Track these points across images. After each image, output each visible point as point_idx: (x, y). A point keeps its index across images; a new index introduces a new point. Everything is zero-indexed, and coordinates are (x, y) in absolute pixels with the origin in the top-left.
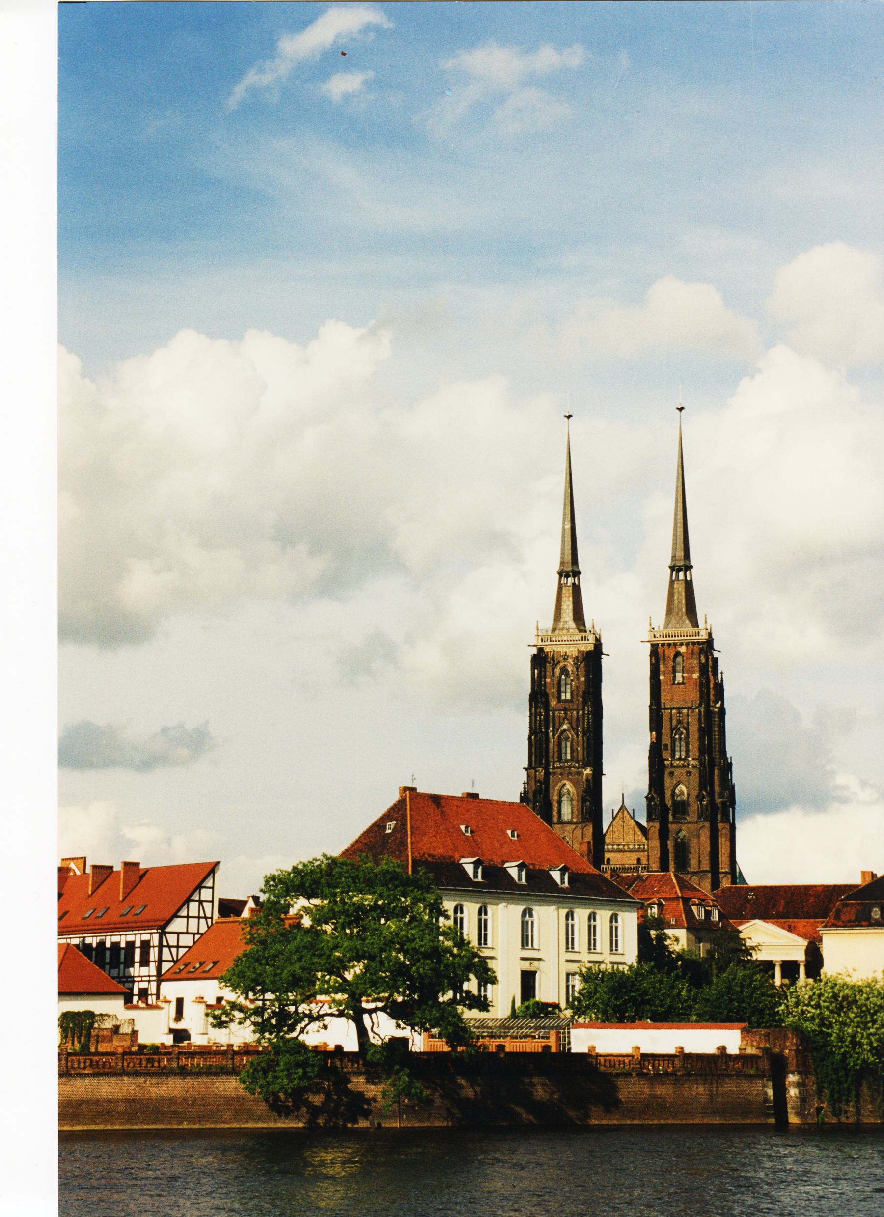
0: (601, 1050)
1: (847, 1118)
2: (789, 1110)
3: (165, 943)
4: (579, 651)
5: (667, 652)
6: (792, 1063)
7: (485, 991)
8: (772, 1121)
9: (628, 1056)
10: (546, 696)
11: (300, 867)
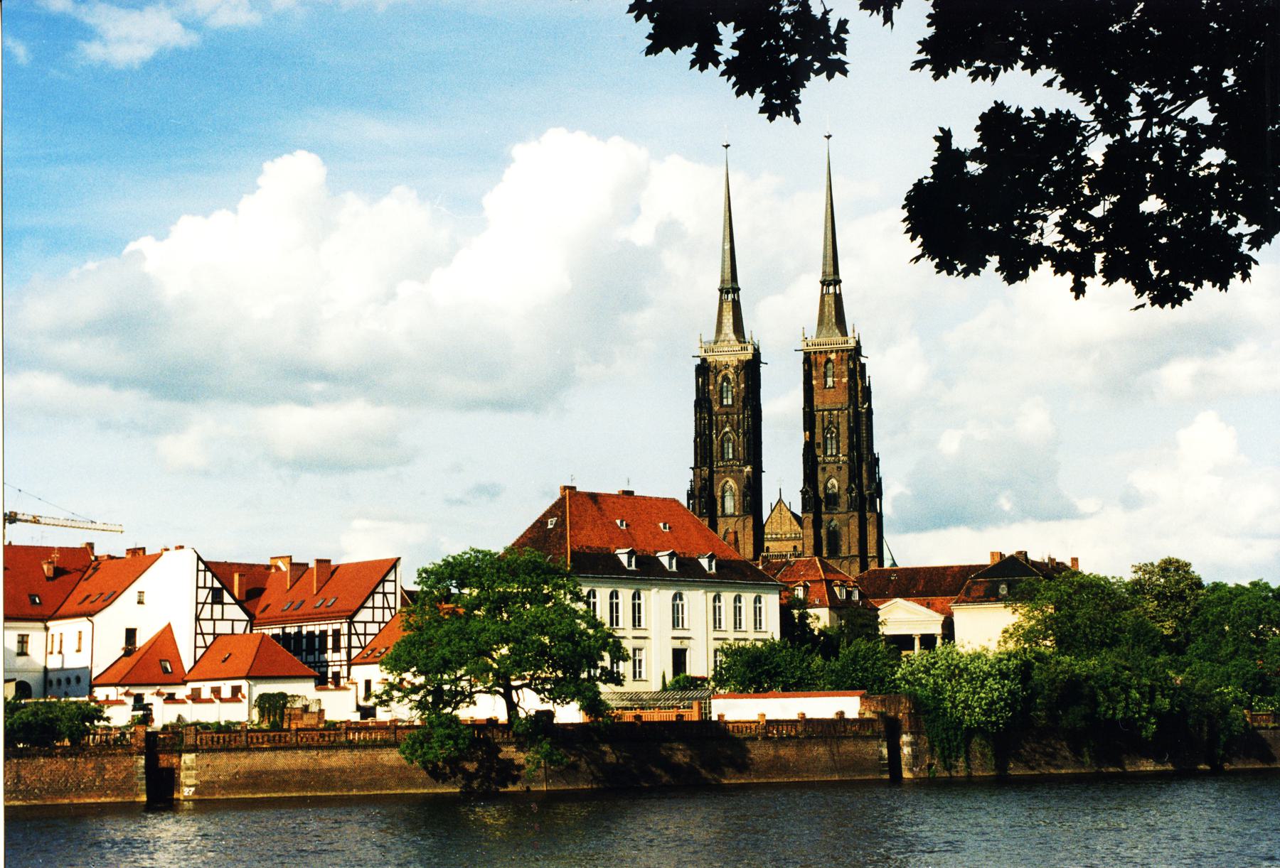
0: (728, 718)
1: (957, 772)
2: (903, 767)
3: (353, 631)
4: (739, 361)
5: (819, 359)
6: (906, 727)
7: (618, 667)
8: (887, 776)
9: (754, 722)
10: (710, 402)
11: (451, 560)
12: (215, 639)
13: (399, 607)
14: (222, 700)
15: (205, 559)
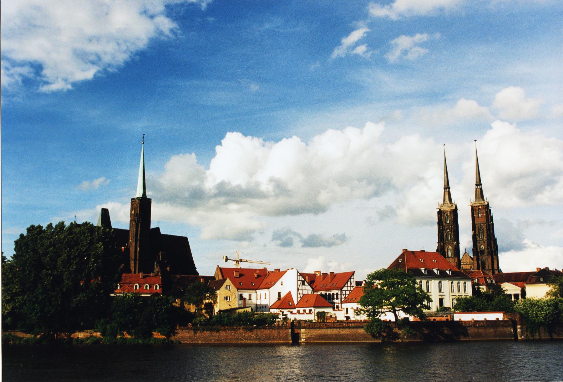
0: (463, 320)
1: (536, 337)
2: (518, 335)
3: (342, 293)
4: (451, 210)
6: (519, 323)
7: (429, 304)
8: (513, 338)
9: (470, 321)
11: (377, 272)
12: (303, 295)
13: (355, 286)
14: (307, 314)
15: (300, 272)
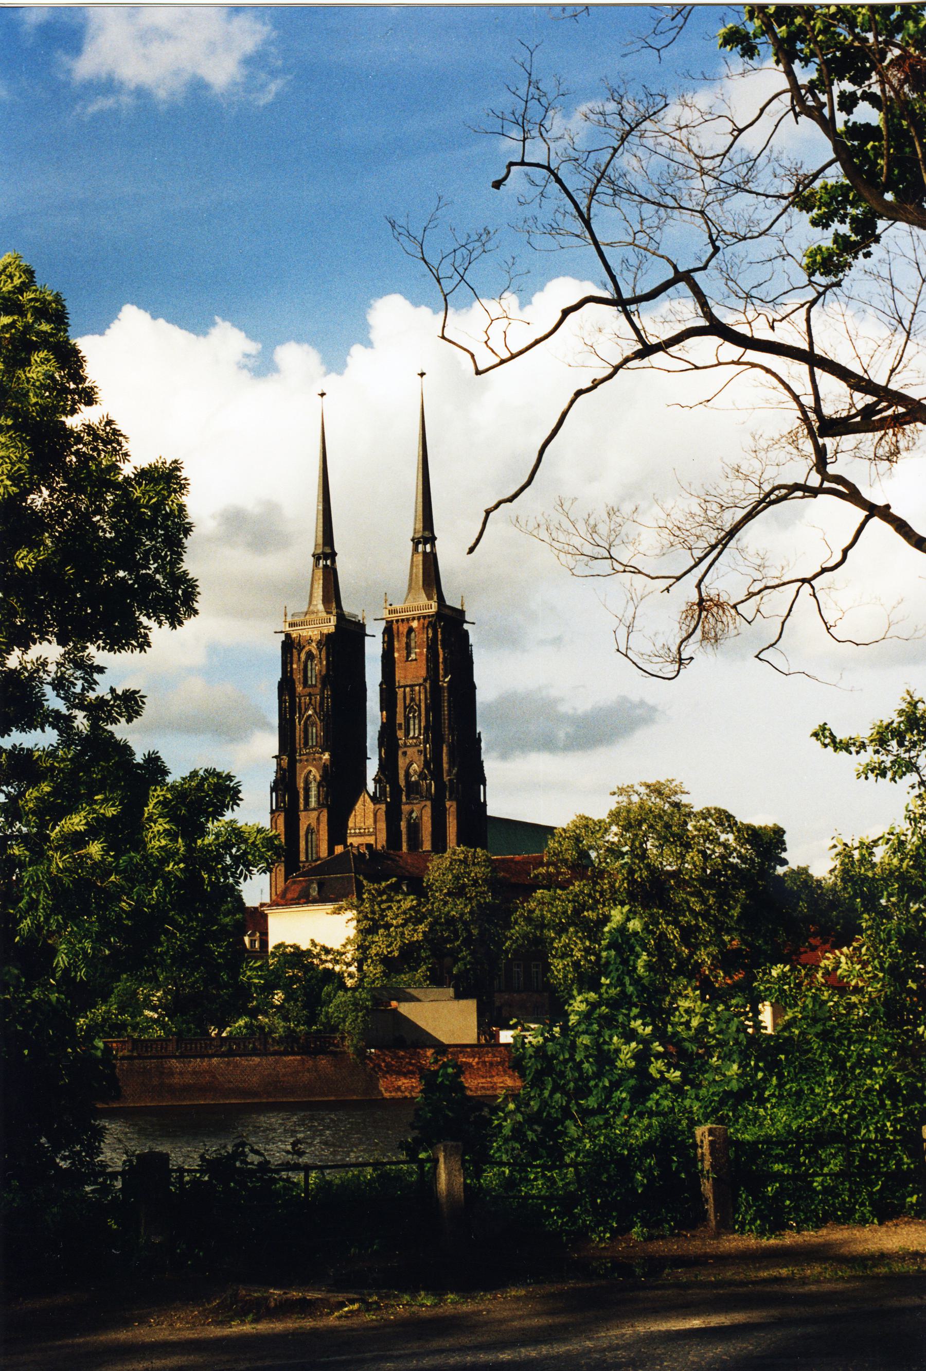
4: (322, 634)
5: (401, 629)
10: (293, 682)
